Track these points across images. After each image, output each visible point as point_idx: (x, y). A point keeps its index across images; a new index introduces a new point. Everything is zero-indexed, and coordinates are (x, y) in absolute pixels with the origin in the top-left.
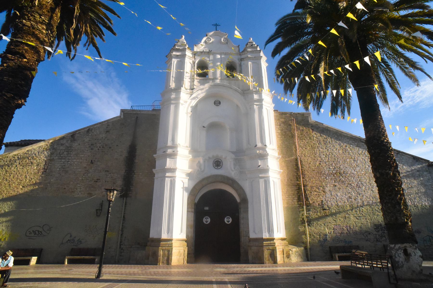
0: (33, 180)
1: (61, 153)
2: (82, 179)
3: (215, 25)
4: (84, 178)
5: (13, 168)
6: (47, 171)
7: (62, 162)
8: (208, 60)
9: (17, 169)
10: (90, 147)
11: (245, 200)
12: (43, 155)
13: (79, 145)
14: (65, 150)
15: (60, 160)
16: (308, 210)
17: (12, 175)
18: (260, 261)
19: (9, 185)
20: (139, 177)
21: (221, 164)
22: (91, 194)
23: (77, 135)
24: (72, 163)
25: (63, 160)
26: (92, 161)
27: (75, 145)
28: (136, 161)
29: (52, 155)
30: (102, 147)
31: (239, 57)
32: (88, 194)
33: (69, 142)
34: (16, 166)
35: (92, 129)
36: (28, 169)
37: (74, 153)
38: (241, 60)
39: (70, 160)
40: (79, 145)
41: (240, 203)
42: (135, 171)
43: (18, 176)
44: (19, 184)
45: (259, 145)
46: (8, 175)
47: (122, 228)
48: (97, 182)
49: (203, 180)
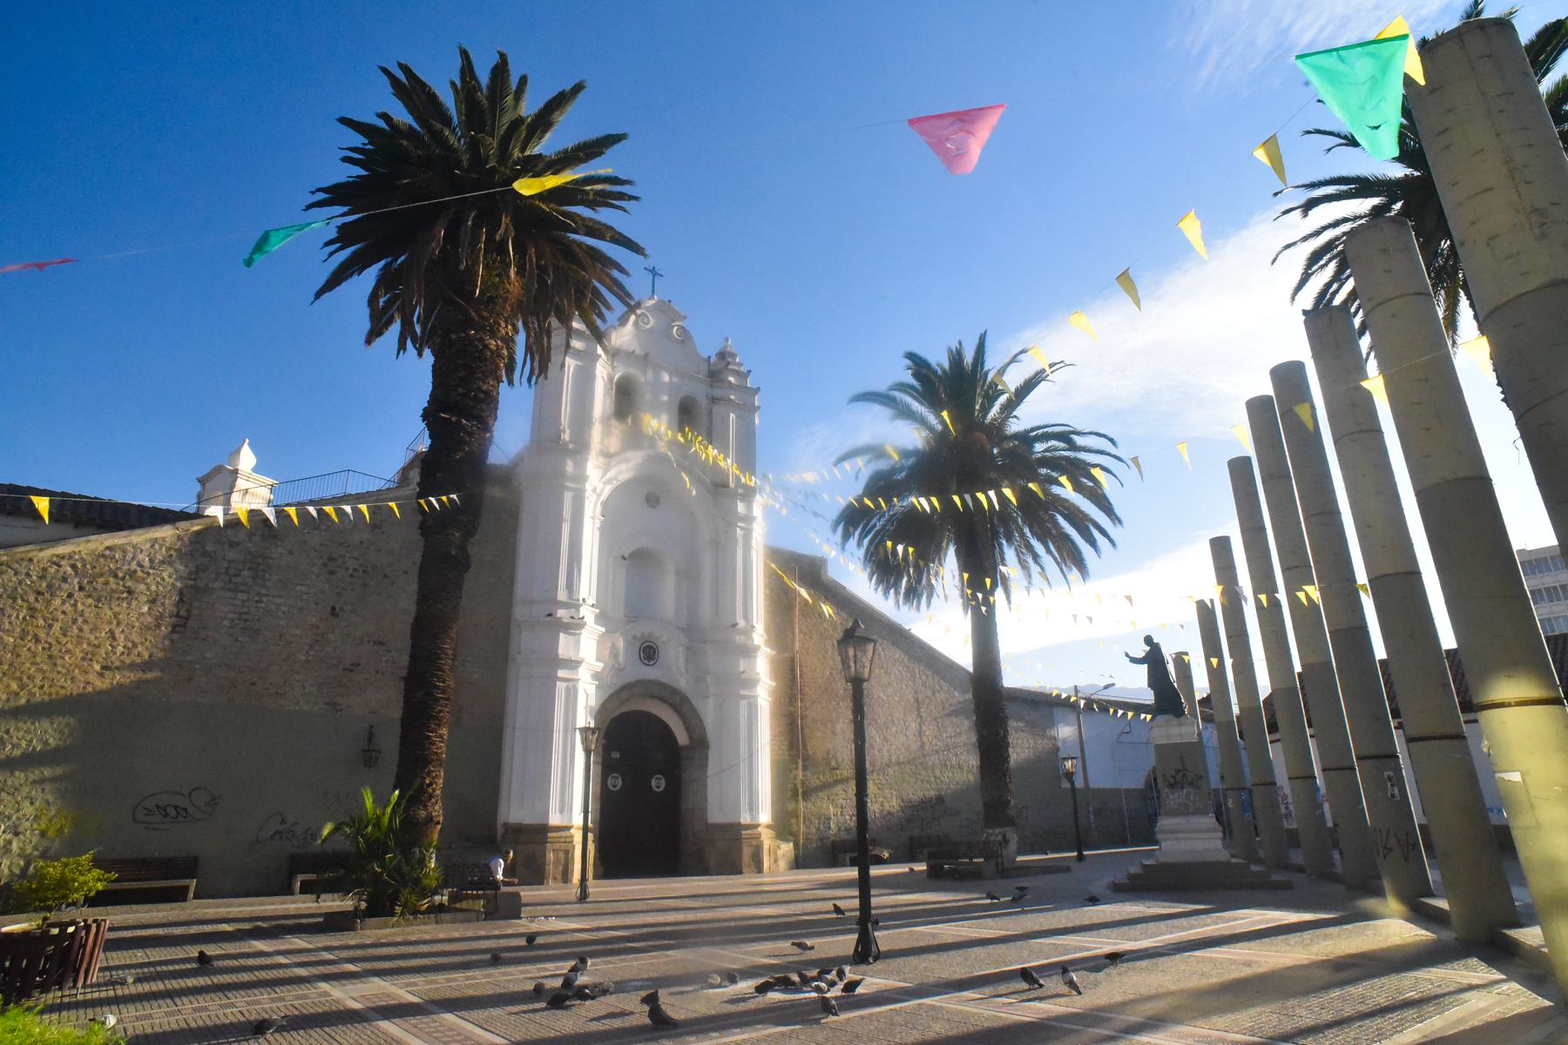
0: (140, 648)
1: (232, 571)
2: (307, 661)
5: (57, 602)
6: (184, 619)
8: (643, 377)
9: (75, 605)
11: (700, 743)
12: (170, 570)
13: (291, 552)
15: (229, 594)
16: (805, 768)
17: (57, 626)
18: (732, 867)
19: (50, 657)
22: (335, 704)
25: (241, 596)
26: (333, 608)
32: (327, 704)
33: (257, 539)
34: (70, 596)
36: (117, 609)
37: (275, 577)
41: (690, 748)
43: (81, 630)
44: (88, 657)
45: (741, 622)
46: (41, 622)
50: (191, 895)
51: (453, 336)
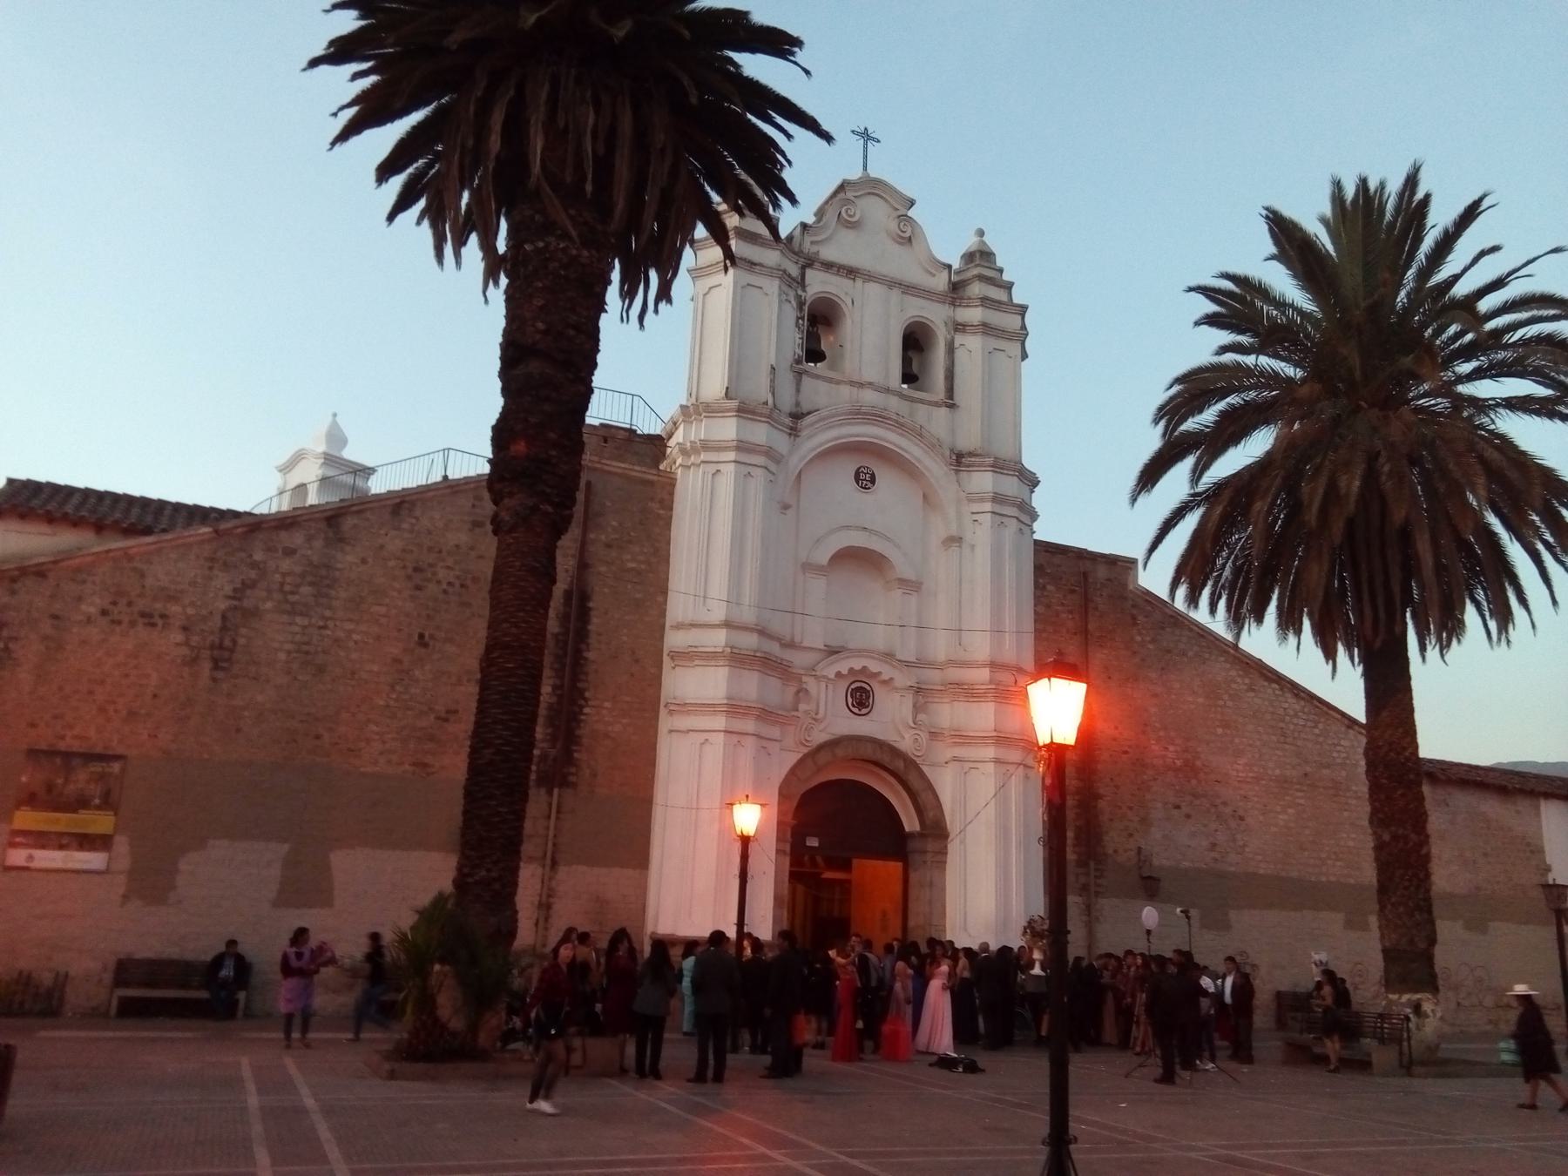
1: (287, 588)
3: (858, 134)
4: (396, 700)
7: (296, 629)
10: (409, 578)
11: (936, 830)
13: (364, 561)
14: (303, 575)
15: (285, 618)
20: (602, 715)
22: (425, 765)
23: (349, 522)
24: (341, 634)
25: (298, 620)
26: (421, 636)
27: (347, 559)
28: (591, 655)
29: (248, 592)
30: (457, 583)
32: (414, 764)
35: (413, 503)
37: (343, 594)
38: (956, 330)
39: (331, 624)
40: (364, 561)
41: (921, 835)
42: (587, 694)
47: (549, 896)
48: (446, 720)
49: (821, 747)
50: (240, 1013)
51: (527, 247)
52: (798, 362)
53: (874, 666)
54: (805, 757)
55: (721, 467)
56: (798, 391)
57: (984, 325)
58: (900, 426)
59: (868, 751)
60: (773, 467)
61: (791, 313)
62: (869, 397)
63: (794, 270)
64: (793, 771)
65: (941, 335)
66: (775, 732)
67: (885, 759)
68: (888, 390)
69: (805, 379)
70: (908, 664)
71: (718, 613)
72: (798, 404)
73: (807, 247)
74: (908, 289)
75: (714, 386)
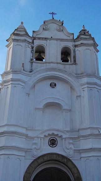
21: (56, 143)
31: (74, 43)
52: (32, 60)
53: (56, 133)
54: (35, 160)
55: (8, 86)
56: (32, 66)
57: (82, 43)
58: (59, 70)
59: (55, 157)
60: (24, 84)
61: (29, 50)
62: (52, 65)
63: (31, 41)
64: (30, 165)
65: (72, 48)
66: (23, 154)
67: (60, 159)
68: (57, 63)
69: (33, 63)
70: (68, 131)
71: (5, 123)
72: (31, 69)
73: (35, 36)
74: (62, 40)
75: (9, 69)
